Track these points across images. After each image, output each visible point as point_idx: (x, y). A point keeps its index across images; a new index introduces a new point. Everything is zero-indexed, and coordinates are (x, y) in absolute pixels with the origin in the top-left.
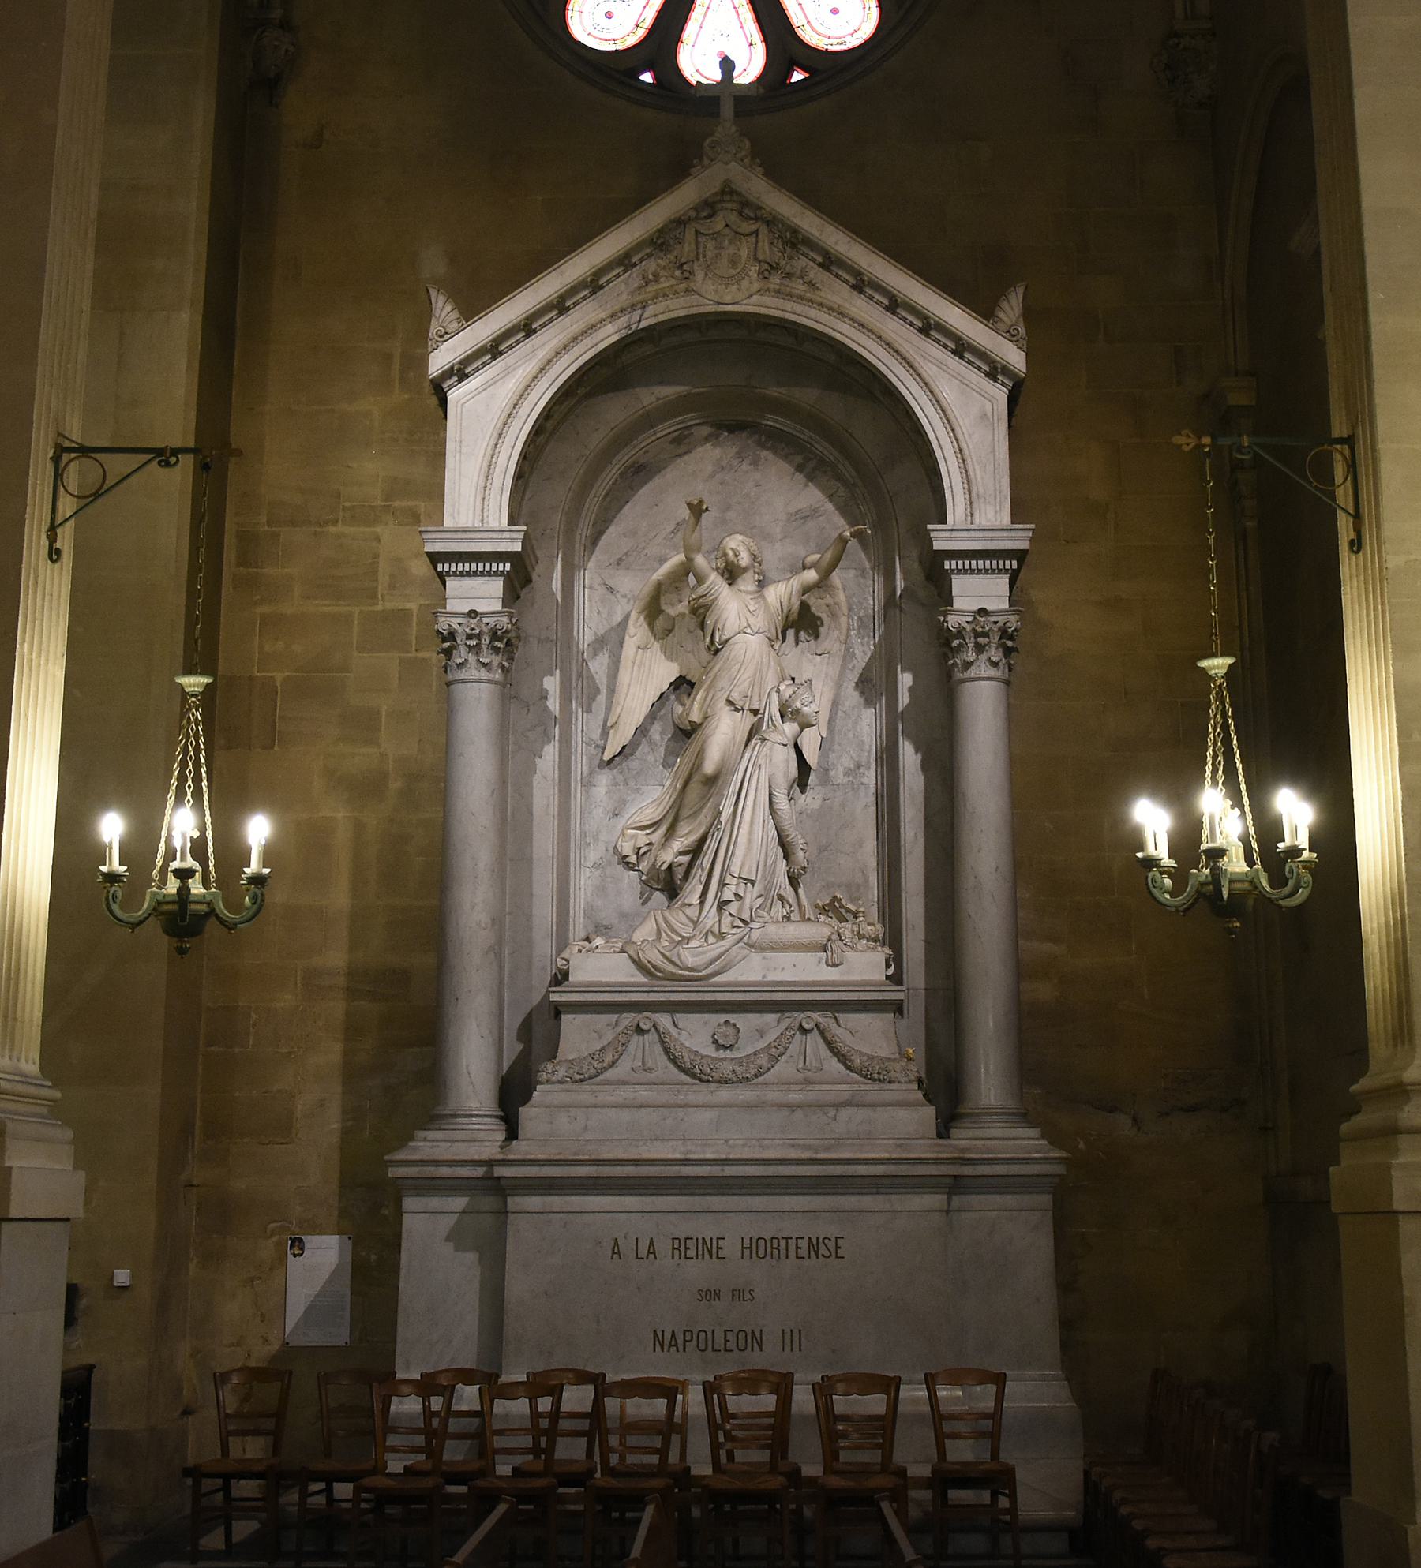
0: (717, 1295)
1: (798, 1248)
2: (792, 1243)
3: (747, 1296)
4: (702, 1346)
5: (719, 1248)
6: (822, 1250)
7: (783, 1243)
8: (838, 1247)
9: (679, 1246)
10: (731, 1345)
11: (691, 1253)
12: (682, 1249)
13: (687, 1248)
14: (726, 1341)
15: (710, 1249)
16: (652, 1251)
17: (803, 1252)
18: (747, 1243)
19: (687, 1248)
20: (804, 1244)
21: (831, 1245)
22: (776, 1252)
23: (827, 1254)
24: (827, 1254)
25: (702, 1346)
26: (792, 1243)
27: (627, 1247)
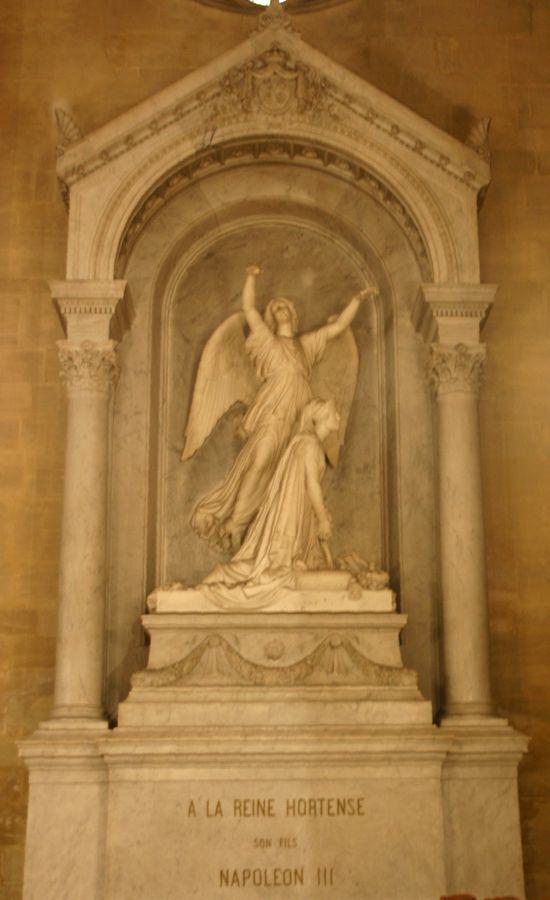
0: (268, 843)
1: (329, 807)
2: (325, 804)
3: (291, 843)
4: (258, 881)
5: (269, 808)
6: (348, 808)
7: (318, 804)
8: (359, 806)
9: (240, 807)
10: (280, 880)
11: (249, 811)
12: (242, 808)
13: (245, 809)
14: (276, 877)
15: (264, 809)
16: (219, 810)
17: (334, 809)
18: (291, 804)
19: (245, 809)
20: (334, 805)
21: (355, 805)
22: (313, 811)
23: (351, 811)
24: (351, 811)
25: (258, 881)
26: (325, 804)
27: (200, 807)
